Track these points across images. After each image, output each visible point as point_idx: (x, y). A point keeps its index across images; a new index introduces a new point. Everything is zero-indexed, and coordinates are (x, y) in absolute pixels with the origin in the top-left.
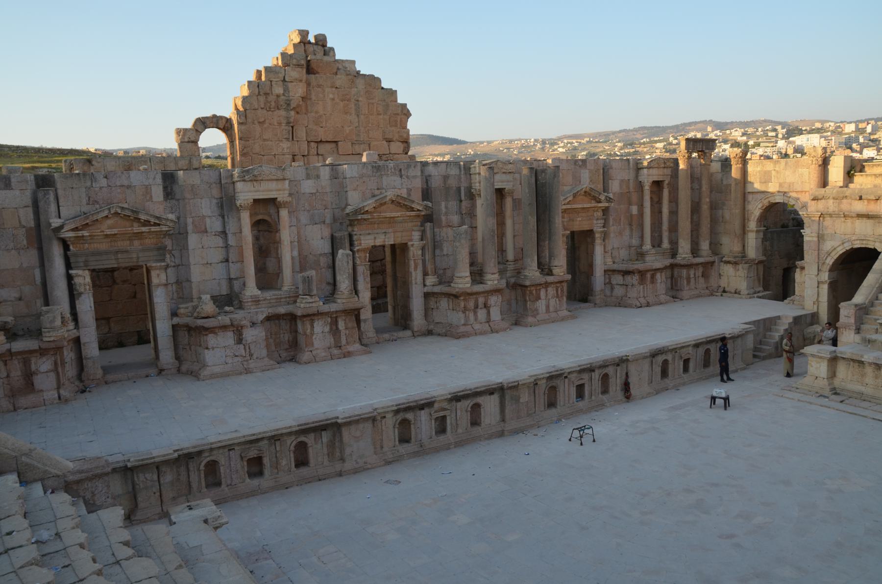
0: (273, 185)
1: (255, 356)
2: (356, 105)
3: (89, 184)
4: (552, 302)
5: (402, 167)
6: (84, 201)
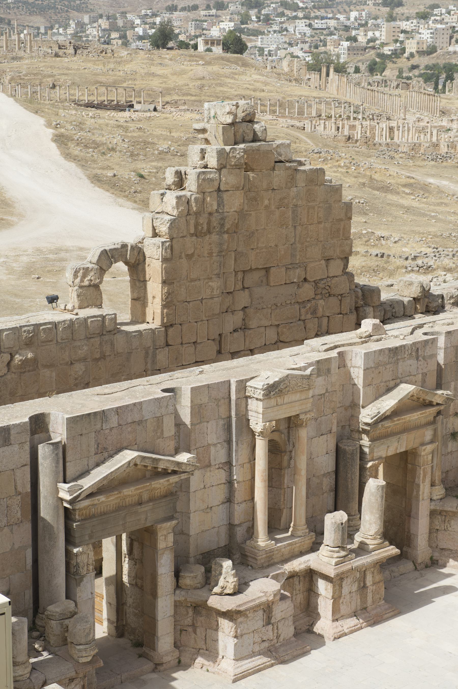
2: (293, 212)
3: (98, 426)
6: (93, 450)
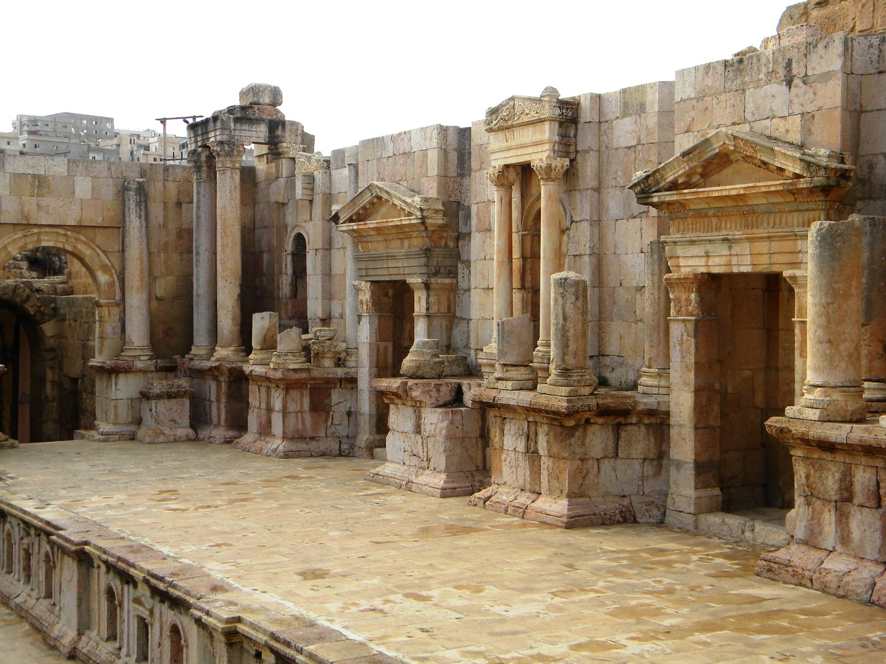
5: (793, 54)
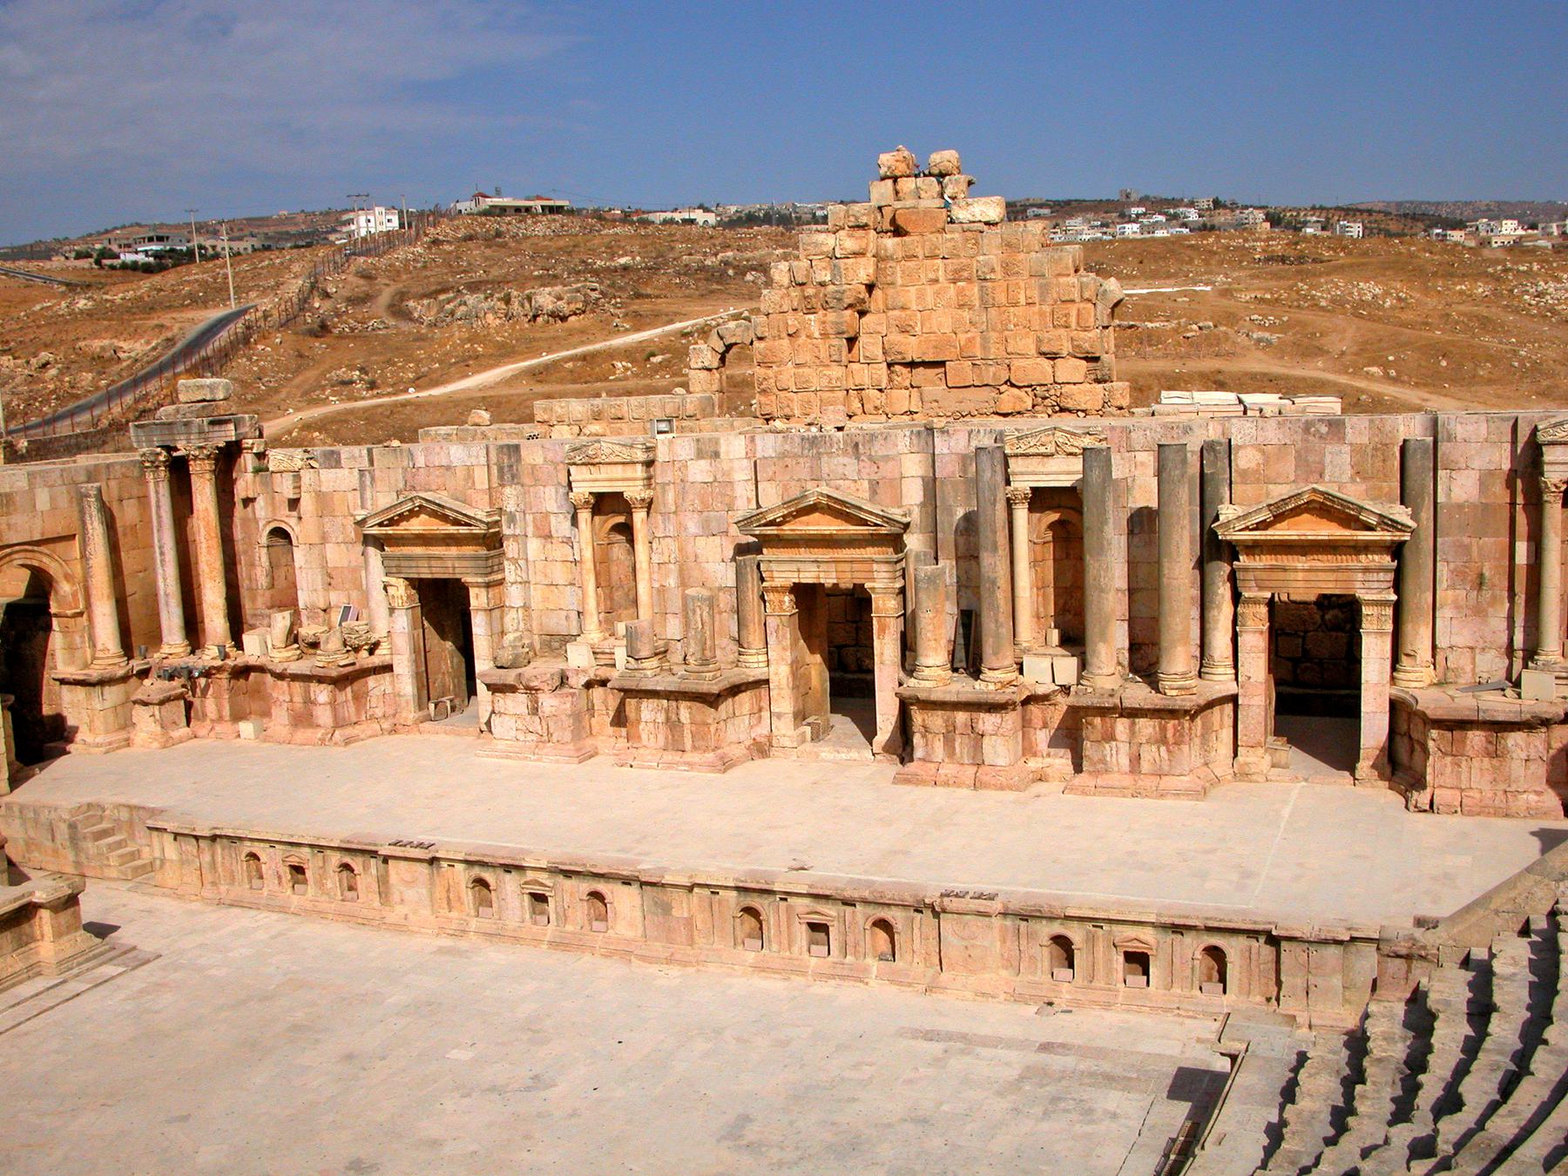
0: (618, 471)
1: (554, 739)
4: (1149, 754)
